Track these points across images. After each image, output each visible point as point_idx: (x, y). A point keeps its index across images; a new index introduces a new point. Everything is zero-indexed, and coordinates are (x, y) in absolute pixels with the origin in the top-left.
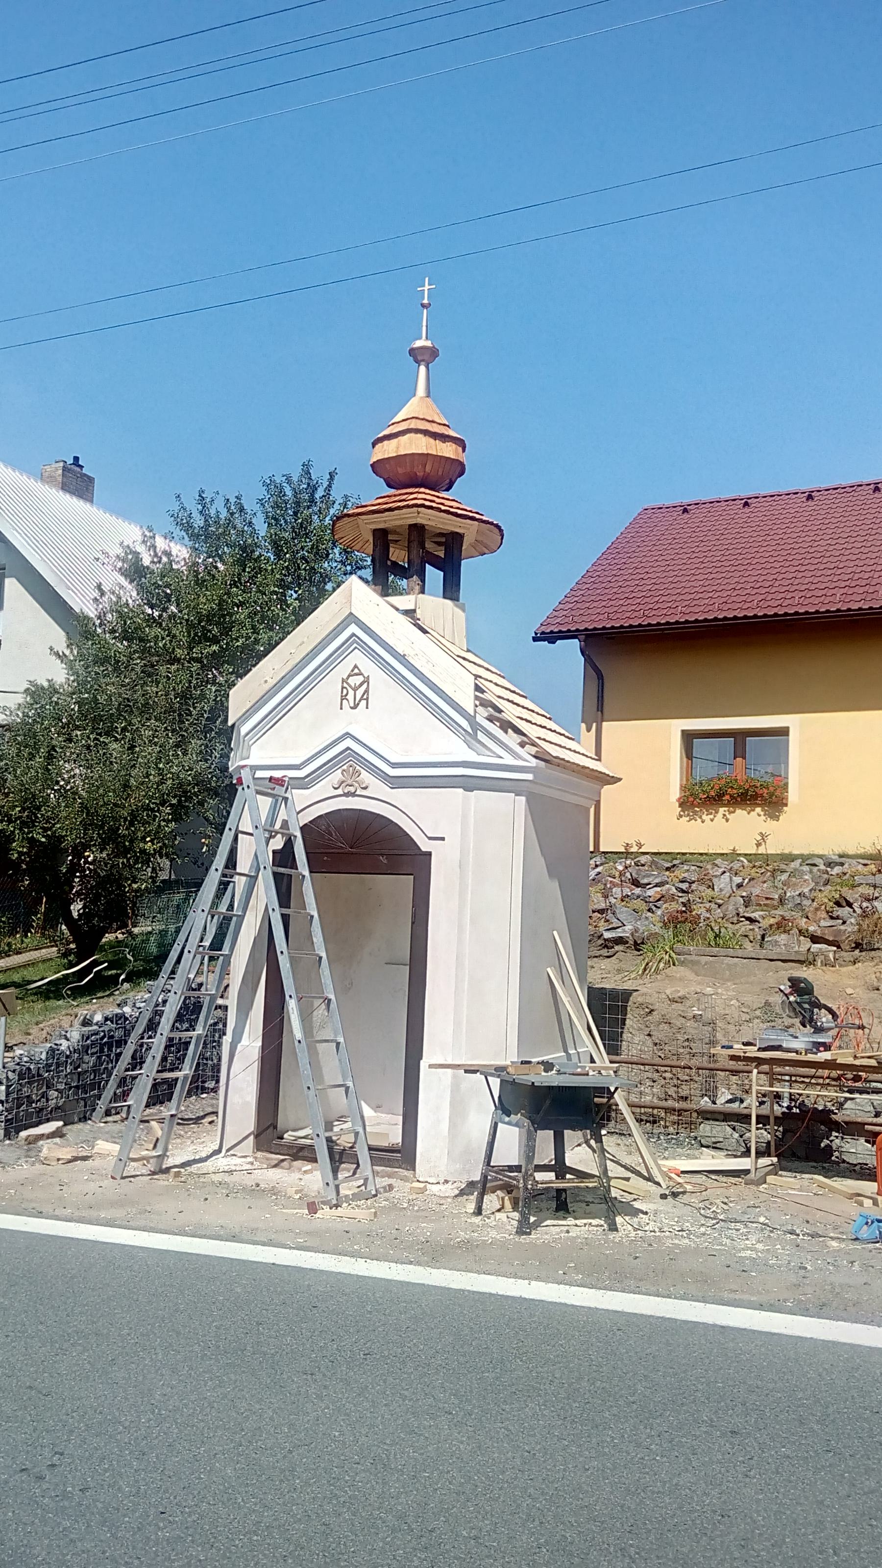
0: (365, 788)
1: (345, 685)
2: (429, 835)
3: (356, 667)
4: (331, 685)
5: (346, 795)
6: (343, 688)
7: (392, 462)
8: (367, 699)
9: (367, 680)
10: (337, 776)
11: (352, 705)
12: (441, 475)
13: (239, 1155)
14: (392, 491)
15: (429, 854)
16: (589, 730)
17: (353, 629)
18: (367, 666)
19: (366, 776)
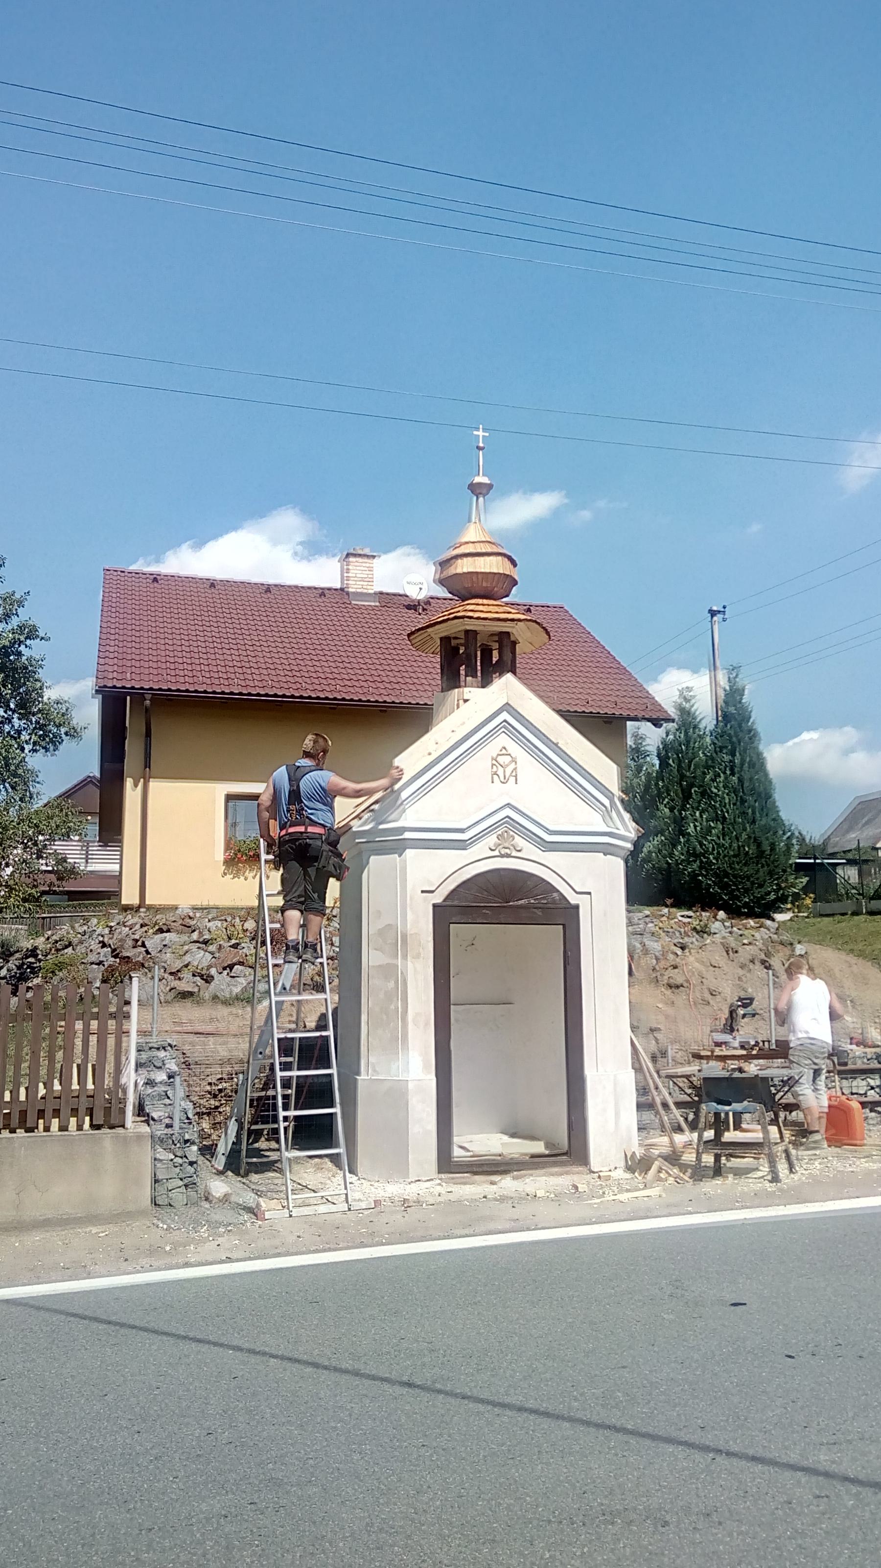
0: (519, 851)
1: (494, 762)
2: (578, 890)
3: (505, 748)
4: (481, 762)
5: (502, 856)
6: (493, 765)
7: (480, 576)
8: (516, 776)
9: (514, 761)
10: (492, 840)
11: (502, 780)
12: (494, 588)
13: (424, 1179)
14: (450, 596)
15: (577, 907)
16: (136, 785)
17: (505, 716)
18: (514, 749)
19: (519, 841)
